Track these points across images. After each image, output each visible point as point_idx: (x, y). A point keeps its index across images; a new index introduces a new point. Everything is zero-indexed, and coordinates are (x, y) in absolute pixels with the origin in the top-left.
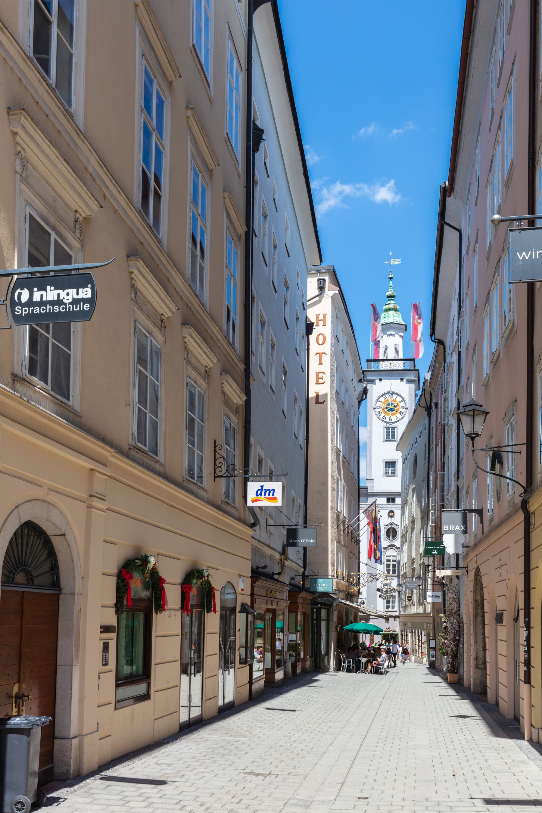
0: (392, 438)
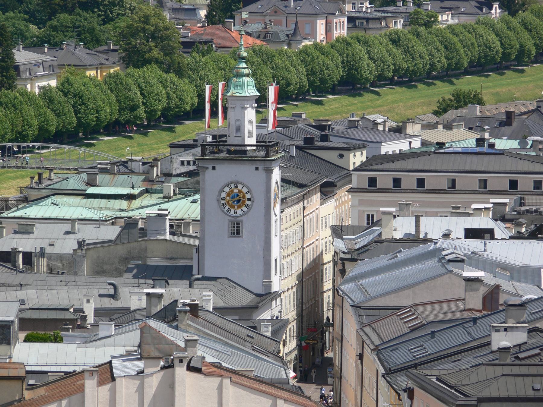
0: (237, 234)
